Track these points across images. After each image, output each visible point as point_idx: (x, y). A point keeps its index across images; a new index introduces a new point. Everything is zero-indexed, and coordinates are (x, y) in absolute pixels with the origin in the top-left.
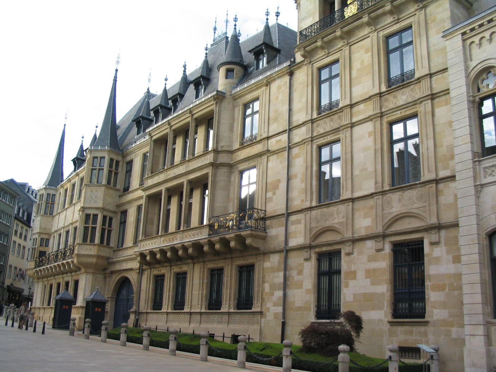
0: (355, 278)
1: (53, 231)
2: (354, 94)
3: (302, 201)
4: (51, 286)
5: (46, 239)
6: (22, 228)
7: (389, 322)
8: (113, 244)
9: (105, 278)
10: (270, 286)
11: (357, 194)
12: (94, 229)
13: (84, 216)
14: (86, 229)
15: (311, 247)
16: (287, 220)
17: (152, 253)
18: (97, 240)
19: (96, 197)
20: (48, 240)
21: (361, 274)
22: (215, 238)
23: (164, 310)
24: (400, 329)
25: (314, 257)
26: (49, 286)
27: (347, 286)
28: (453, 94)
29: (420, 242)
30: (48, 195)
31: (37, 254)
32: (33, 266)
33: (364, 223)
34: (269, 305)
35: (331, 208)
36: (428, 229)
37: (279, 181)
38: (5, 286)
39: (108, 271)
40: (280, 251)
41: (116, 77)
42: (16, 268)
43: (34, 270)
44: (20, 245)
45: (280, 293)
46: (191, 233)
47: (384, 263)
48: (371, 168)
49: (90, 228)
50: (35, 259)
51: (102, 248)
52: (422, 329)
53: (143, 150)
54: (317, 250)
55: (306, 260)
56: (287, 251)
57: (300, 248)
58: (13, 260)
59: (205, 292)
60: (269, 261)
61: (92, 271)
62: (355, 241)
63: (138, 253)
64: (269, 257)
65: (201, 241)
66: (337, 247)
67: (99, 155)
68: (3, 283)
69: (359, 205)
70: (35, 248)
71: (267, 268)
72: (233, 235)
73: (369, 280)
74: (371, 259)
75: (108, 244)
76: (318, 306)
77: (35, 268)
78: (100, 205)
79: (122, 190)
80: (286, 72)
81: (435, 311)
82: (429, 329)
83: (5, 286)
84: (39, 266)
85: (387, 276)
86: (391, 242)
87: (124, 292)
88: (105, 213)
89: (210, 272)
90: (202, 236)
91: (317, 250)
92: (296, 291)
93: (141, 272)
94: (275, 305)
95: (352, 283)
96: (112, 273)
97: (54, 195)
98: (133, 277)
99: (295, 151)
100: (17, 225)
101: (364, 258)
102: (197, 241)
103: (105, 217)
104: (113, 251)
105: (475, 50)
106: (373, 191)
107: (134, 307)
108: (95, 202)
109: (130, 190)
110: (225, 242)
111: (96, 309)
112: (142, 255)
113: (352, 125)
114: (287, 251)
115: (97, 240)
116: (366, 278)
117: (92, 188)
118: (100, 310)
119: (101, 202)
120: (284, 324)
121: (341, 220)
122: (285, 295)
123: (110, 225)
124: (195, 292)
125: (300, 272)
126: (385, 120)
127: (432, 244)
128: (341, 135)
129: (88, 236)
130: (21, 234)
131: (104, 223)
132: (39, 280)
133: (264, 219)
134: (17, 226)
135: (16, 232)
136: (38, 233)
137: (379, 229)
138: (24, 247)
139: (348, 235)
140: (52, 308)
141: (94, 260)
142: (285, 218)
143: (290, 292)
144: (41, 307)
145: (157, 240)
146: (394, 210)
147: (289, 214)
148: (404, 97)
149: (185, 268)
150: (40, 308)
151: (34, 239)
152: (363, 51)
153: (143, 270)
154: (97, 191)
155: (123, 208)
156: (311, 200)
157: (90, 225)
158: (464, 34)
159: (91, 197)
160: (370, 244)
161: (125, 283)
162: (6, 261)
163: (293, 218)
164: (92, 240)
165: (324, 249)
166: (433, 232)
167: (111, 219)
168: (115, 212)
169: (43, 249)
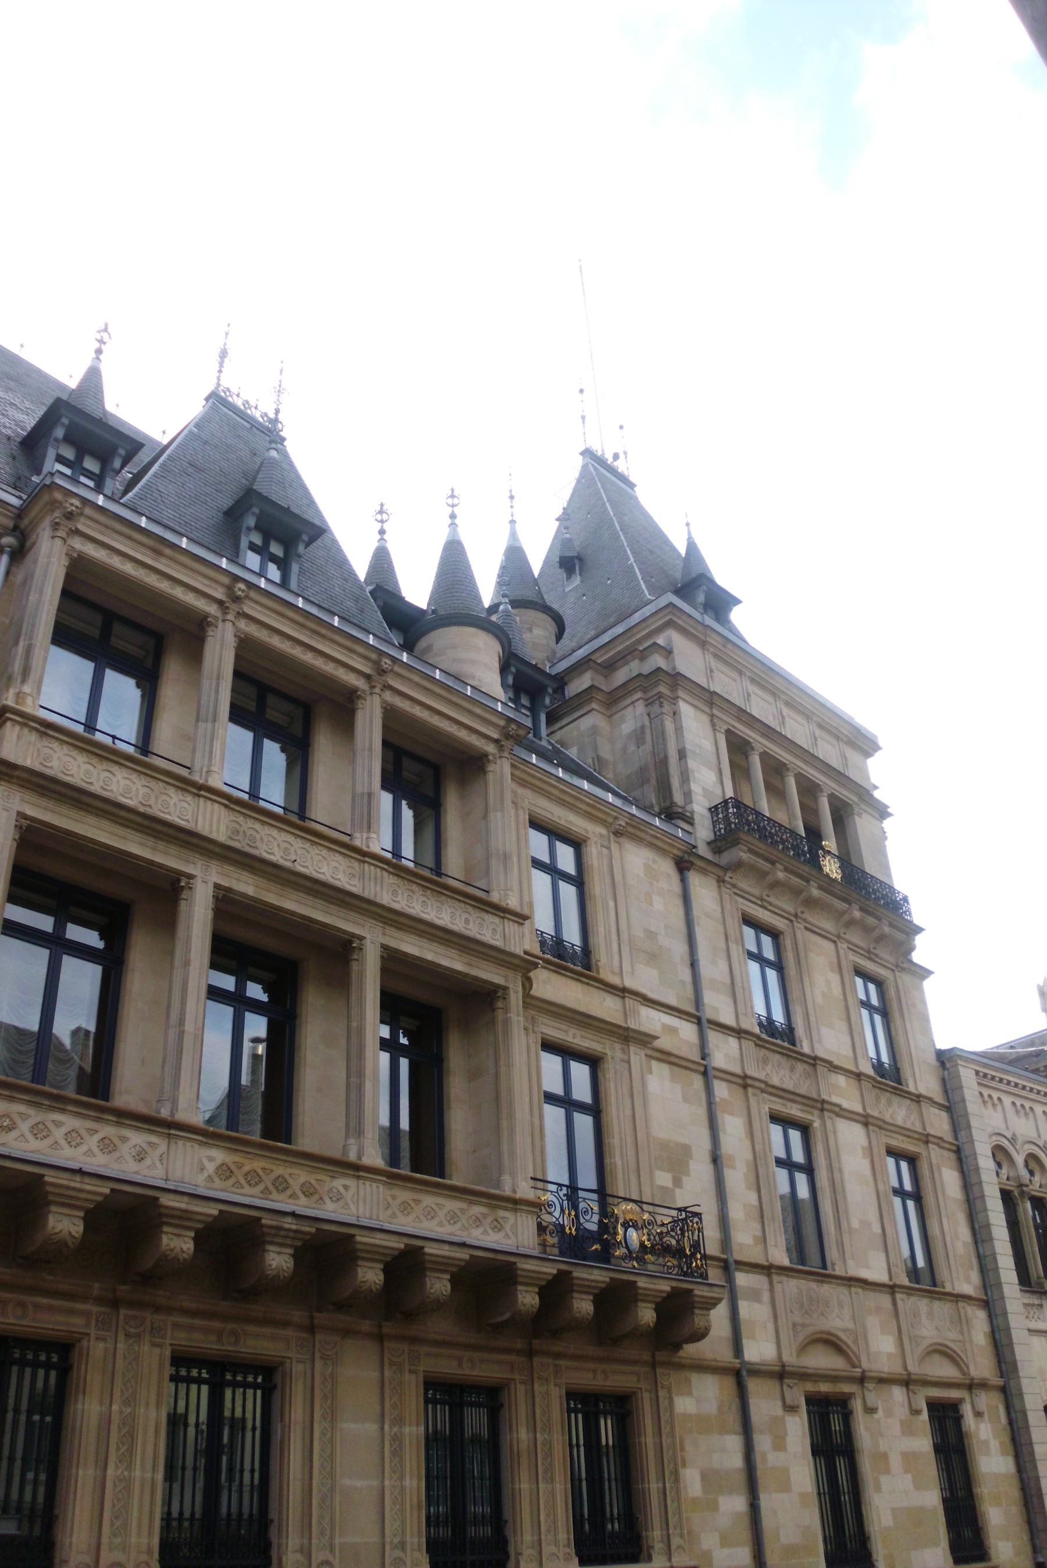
10: (705, 1477)
21: (895, 1462)
27: (878, 1489)
35: (826, 1287)
54: (810, 1387)
55: (790, 1409)
56: (739, 1375)
60: (690, 1393)
64: (688, 1381)
71: (687, 1416)
73: (909, 1476)
80: (675, 851)
95: (884, 1480)
102: (500, 1257)
116: (906, 1471)
122: (754, 1507)
125: (779, 1444)
143: (766, 1501)
145: (162, 1144)
165: (824, 1388)
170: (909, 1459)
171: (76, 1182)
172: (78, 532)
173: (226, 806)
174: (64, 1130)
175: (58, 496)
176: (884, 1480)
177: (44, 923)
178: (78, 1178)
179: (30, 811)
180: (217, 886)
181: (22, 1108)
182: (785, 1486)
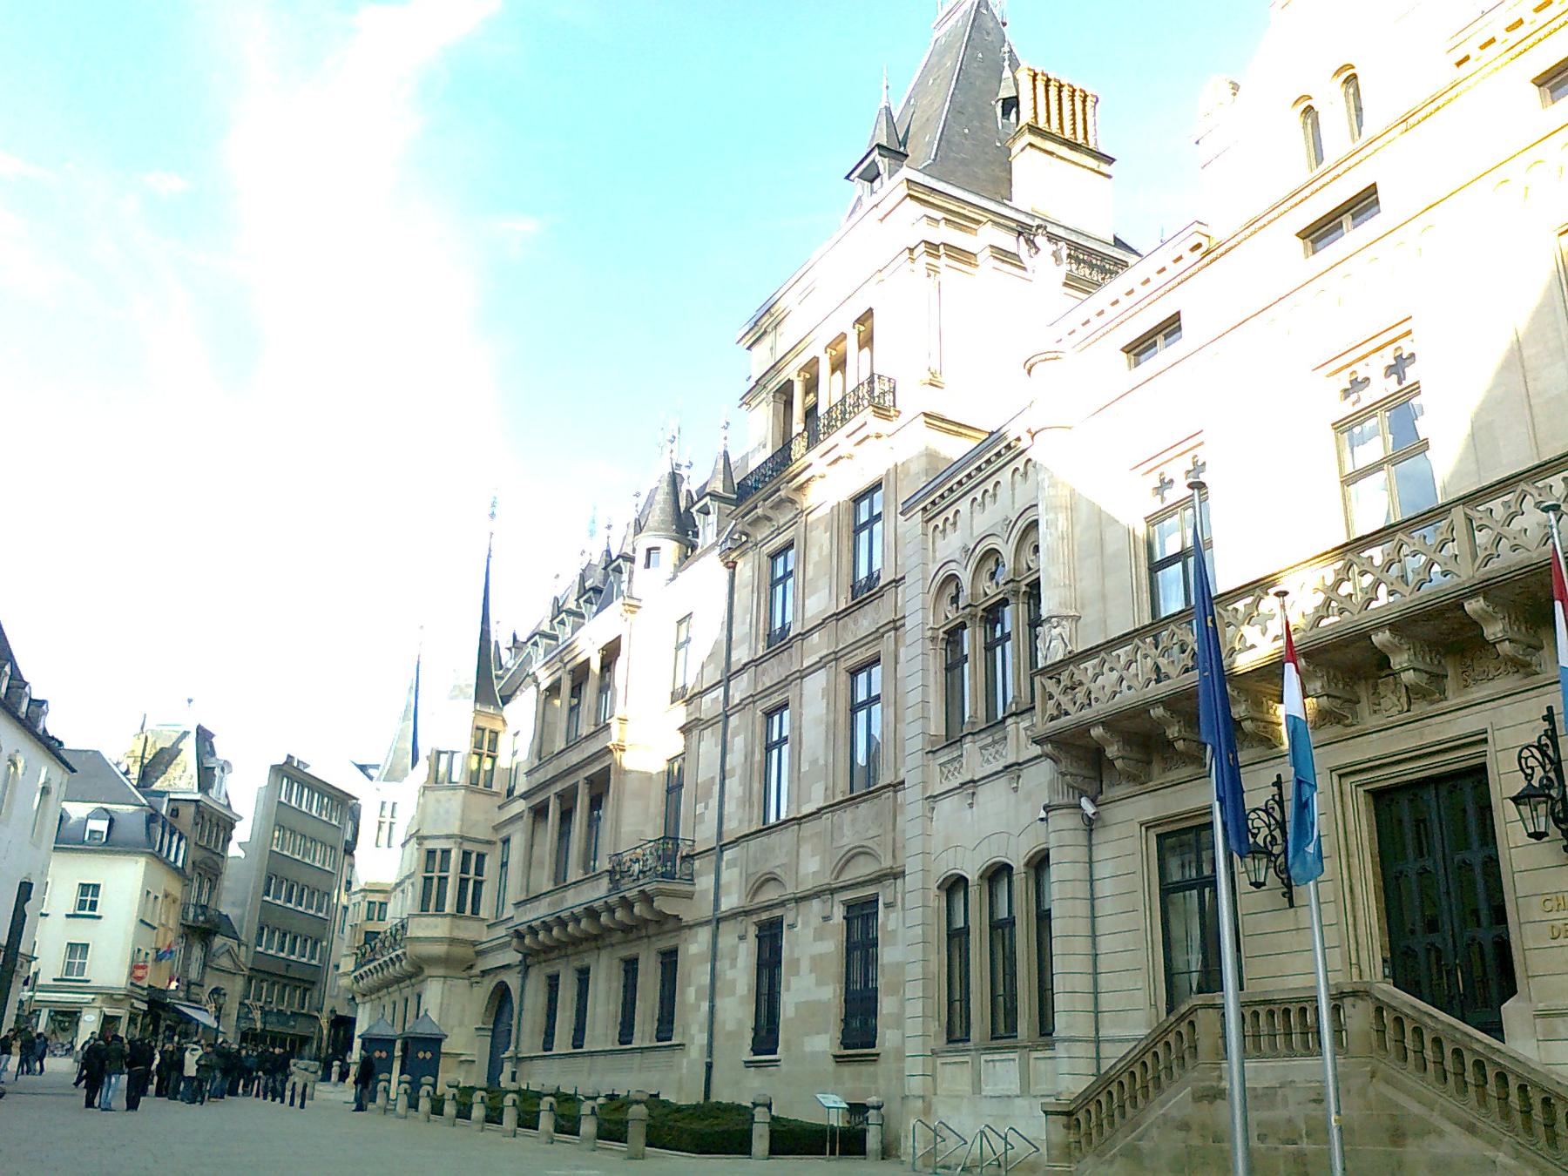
0: (797, 973)
2: (808, 614)
3: (740, 822)
7: (838, 1059)
8: (485, 911)
11: (806, 810)
12: (443, 880)
13: (424, 854)
14: (428, 880)
15: (747, 913)
16: (720, 859)
17: (533, 931)
18: (448, 909)
19: (447, 812)
20: (383, 905)
21: (805, 965)
22: (613, 899)
23: (554, 1052)
24: (847, 1070)
25: (753, 931)
27: (788, 990)
28: (909, 623)
29: (873, 902)
33: (812, 868)
34: (694, 1029)
36: (879, 879)
37: (713, 778)
39: (476, 971)
40: (707, 922)
45: (705, 1006)
46: (585, 887)
47: (832, 946)
48: (822, 762)
49: (435, 881)
51: (461, 922)
52: (871, 1068)
55: (742, 938)
57: (734, 915)
59: (612, 1007)
61: (441, 972)
62: (799, 900)
65: (596, 904)
66: (777, 912)
69: (808, 828)
72: (635, 892)
74: (819, 936)
75: (475, 911)
76: (756, 1030)
78: (456, 831)
79: (505, 792)
81: (889, 1032)
82: (881, 1068)
85: (836, 967)
86: (844, 903)
87: (505, 1018)
88: (468, 846)
89: (622, 965)
90: (599, 891)
91: (755, 918)
92: (727, 1000)
93: (525, 968)
94: (701, 1031)
95: (794, 980)
96: (484, 973)
98: (512, 980)
99: (734, 721)
101: (810, 933)
103: (466, 854)
105: (940, 543)
106: (822, 804)
107: (512, 1048)
110: (627, 904)
111: (421, 1055)
112: (519, 935)
113: (803, 674)
114: (718, 921)
115: (450, 905)
118: (429, 1055)
119: (458, 823)
120: (709, 1066)
121: (785, 860)
123: (479, 872)
124: (600, 1010)
125: (733, 965)
126: (843, 665)
127: (887, 906)
128: (791, 694)
129: (430, 897)
131: (464, 869)
133: (689, 857)
137: (826, 879)
139: (790, 890)
141: (440, 950)
142: (714, 858)
143: (719, 1003)
146: (845, 841)
147: (722, 848)
148: (866, 623)
149: (588, 960)
152: (822, 528)
153: (527, 967)
155: (504, 833)
156: (750, 821)
157: (436, 874)
158: (925, 509)
160: (816, 904)
161: (502, 995)
163: (727, 855)
164: (440, 906)
165: (764, 916)
166: (887, 883)
167: (481, 857)
168: (489, 842)
169: (371, 927)
170: (816, 961)
176: (794, 982)
182: (733, 993)
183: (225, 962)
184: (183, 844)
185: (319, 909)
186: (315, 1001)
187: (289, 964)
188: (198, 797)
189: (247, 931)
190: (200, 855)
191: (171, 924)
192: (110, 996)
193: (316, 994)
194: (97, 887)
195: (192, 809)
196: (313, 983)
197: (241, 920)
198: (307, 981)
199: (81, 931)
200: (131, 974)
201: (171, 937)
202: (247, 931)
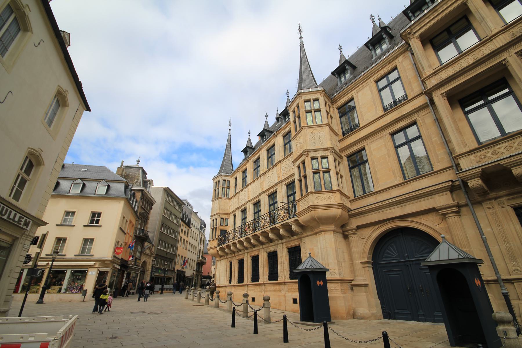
1: (231, 211)
4: (241, 263)
5: (226, 219)
6: (186, 228)
9: (346, 237)
19: (320, 137)
26: (237, 262)
30: (224, 180)
31: (218, 233)
32: (216, 245)
38: (176, 270)
41: (302, 45)
42: (182, 256)
43: (218, 248)
44: (184, 240)
50: (217, 237)
53: (373, 78)
58: (180, 250)
61: (332, 227)
63: (479, 170)
67: (311, 97)
68: (174, 269)
70: (216, 228)
77: (218, 246)
78: (328, 145)
83: (176, 270)
84: (225, 243)
96: (359, 227)
97: (229, 181)
100: (183, 225)
103: (335, 160)
104: (350, 201)
108: (321, 143)
109: (361, 126)
117: (312, 129)
130: (185, 232)
132: (222, 258)
134: (183, 227)
135: (182, 230)
136: (218, 213)
138: (187, 242)
140: (247, 285)
141: (338, 212)
144: (227, 285)
150: (226, 286)
151: (213, 221)
154: (319, 132)
159: (314, 138)
162: (176, 252)
171: (513, 159)
172: (415, 33)
173: (504, 33)
174: (503, 149)
175: (404, 34)
177: (482, 102)
178: (512, 158)
179: (443, 92)
180: (516, 53)
181: (485, 151)
183: (148, 251)
184: (137, 204)
185: (175, 236)
186: (173, 266)
187: (167, 253)
188: (143, 189)
189: (155, 241)
190: (142, 211)
191: (131, 234)
192: (103, 262)
193: (173, 263)
194: (99, 214)
195: (140, 193)
196: (173, 260)
197: (153, 237)
198: (170, 259)
199: (91, 233)
200: (115, 252)
201: (131, 239)
202: (155, 241)
